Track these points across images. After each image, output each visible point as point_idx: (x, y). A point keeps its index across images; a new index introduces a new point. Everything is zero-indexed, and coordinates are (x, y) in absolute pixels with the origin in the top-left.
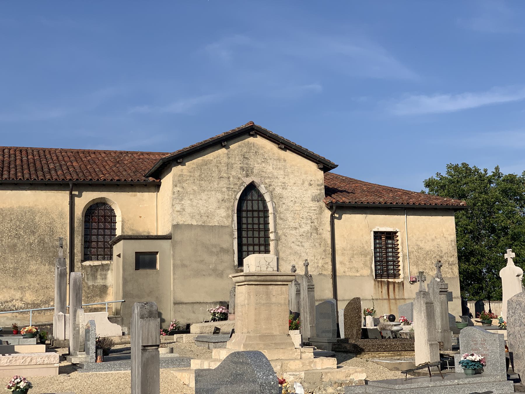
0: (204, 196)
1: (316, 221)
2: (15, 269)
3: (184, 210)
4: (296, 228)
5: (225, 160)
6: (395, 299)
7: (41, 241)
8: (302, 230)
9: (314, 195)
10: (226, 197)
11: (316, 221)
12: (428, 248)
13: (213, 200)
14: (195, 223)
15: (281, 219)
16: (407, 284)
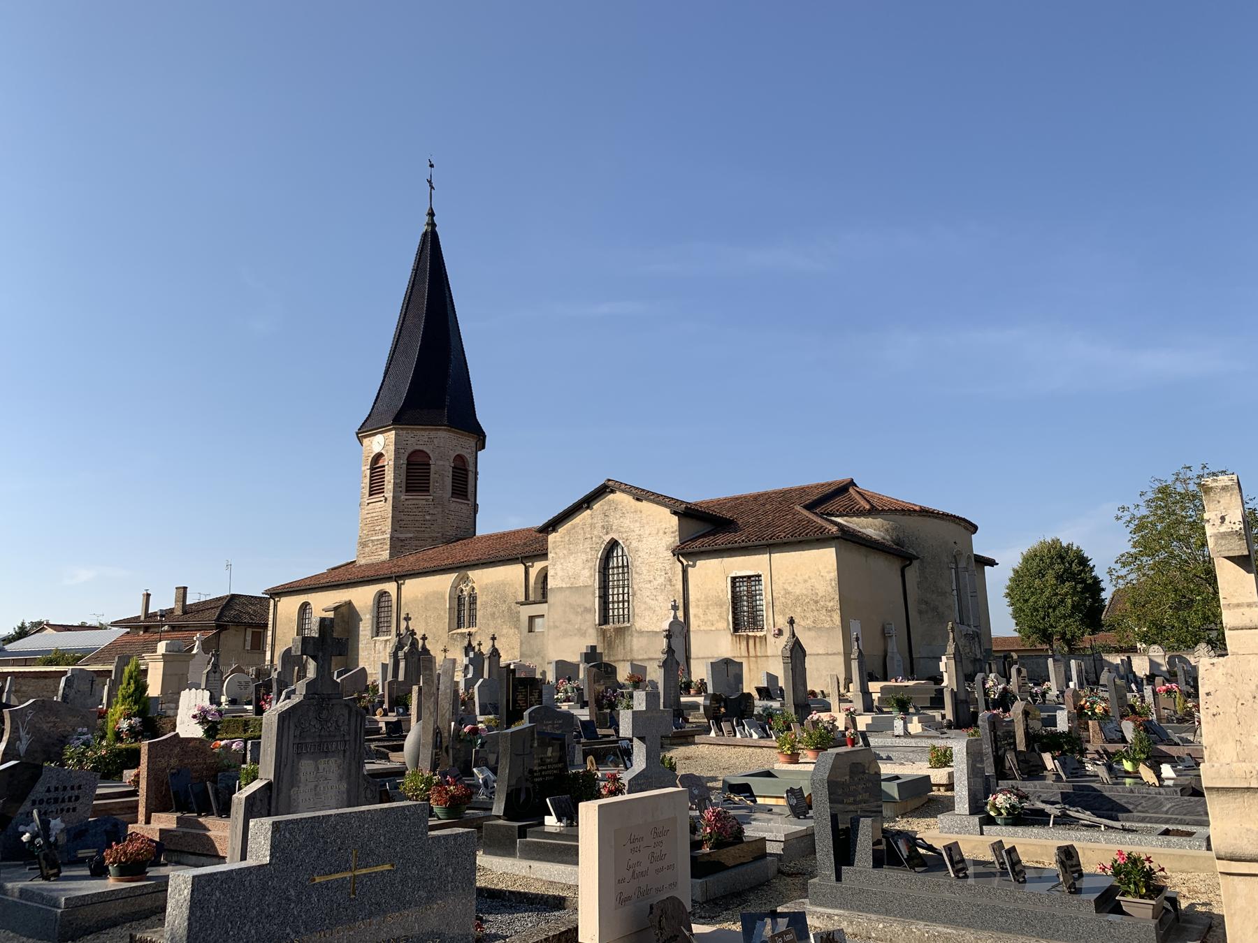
0: (572, 559)
5: (590, 521)
6: (756, 657)
8: (656, 583)
12: (798, 592)
13: (579, 561)
16: (770, 639)
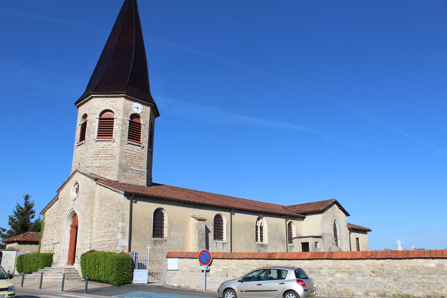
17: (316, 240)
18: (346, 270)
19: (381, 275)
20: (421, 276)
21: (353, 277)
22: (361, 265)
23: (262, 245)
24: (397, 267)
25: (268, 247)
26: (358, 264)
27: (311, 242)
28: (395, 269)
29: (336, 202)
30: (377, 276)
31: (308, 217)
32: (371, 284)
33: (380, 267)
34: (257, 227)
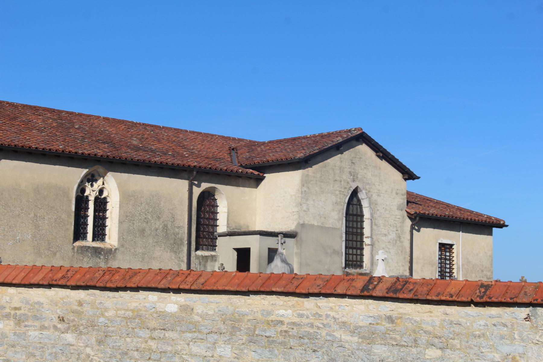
1: (399, 229)
2: (144, 254)
3: (308, 209)
4: (386, 235)
7: (165, 226)
9: (399, 203)
10: (339, 200)
11: (399, 229)
14: (316, 224)
15: (376, 225)
17: (271, 242)
18: (13, 312)
19: (75, 329)
20: (144, 334)
21: (24, 329)
22: (42, 300)
23: (97, 251)
24: (106, 309)
25: (119, 256)
26: (36, 299)
27: (257, 246)
28: (103, 315)
29: (362, 138)
30: (66, 331)
31: (270, 178)
32: (54, 350)
33: (76, 307)
34: (81, 201)
